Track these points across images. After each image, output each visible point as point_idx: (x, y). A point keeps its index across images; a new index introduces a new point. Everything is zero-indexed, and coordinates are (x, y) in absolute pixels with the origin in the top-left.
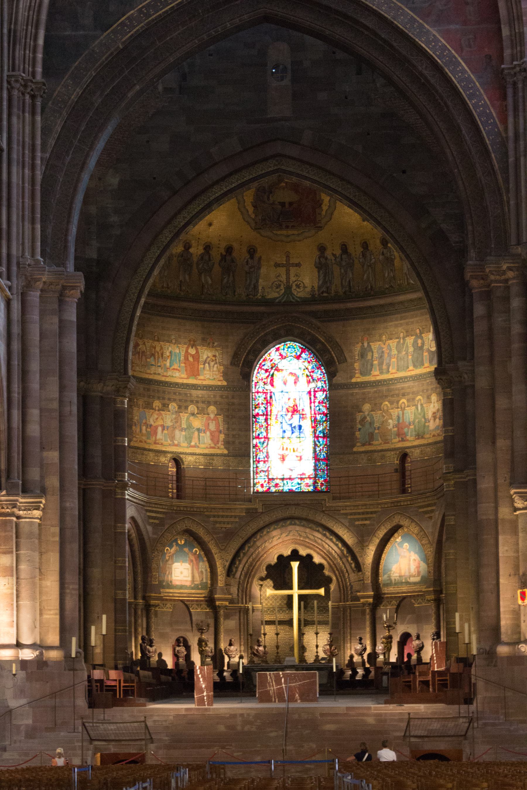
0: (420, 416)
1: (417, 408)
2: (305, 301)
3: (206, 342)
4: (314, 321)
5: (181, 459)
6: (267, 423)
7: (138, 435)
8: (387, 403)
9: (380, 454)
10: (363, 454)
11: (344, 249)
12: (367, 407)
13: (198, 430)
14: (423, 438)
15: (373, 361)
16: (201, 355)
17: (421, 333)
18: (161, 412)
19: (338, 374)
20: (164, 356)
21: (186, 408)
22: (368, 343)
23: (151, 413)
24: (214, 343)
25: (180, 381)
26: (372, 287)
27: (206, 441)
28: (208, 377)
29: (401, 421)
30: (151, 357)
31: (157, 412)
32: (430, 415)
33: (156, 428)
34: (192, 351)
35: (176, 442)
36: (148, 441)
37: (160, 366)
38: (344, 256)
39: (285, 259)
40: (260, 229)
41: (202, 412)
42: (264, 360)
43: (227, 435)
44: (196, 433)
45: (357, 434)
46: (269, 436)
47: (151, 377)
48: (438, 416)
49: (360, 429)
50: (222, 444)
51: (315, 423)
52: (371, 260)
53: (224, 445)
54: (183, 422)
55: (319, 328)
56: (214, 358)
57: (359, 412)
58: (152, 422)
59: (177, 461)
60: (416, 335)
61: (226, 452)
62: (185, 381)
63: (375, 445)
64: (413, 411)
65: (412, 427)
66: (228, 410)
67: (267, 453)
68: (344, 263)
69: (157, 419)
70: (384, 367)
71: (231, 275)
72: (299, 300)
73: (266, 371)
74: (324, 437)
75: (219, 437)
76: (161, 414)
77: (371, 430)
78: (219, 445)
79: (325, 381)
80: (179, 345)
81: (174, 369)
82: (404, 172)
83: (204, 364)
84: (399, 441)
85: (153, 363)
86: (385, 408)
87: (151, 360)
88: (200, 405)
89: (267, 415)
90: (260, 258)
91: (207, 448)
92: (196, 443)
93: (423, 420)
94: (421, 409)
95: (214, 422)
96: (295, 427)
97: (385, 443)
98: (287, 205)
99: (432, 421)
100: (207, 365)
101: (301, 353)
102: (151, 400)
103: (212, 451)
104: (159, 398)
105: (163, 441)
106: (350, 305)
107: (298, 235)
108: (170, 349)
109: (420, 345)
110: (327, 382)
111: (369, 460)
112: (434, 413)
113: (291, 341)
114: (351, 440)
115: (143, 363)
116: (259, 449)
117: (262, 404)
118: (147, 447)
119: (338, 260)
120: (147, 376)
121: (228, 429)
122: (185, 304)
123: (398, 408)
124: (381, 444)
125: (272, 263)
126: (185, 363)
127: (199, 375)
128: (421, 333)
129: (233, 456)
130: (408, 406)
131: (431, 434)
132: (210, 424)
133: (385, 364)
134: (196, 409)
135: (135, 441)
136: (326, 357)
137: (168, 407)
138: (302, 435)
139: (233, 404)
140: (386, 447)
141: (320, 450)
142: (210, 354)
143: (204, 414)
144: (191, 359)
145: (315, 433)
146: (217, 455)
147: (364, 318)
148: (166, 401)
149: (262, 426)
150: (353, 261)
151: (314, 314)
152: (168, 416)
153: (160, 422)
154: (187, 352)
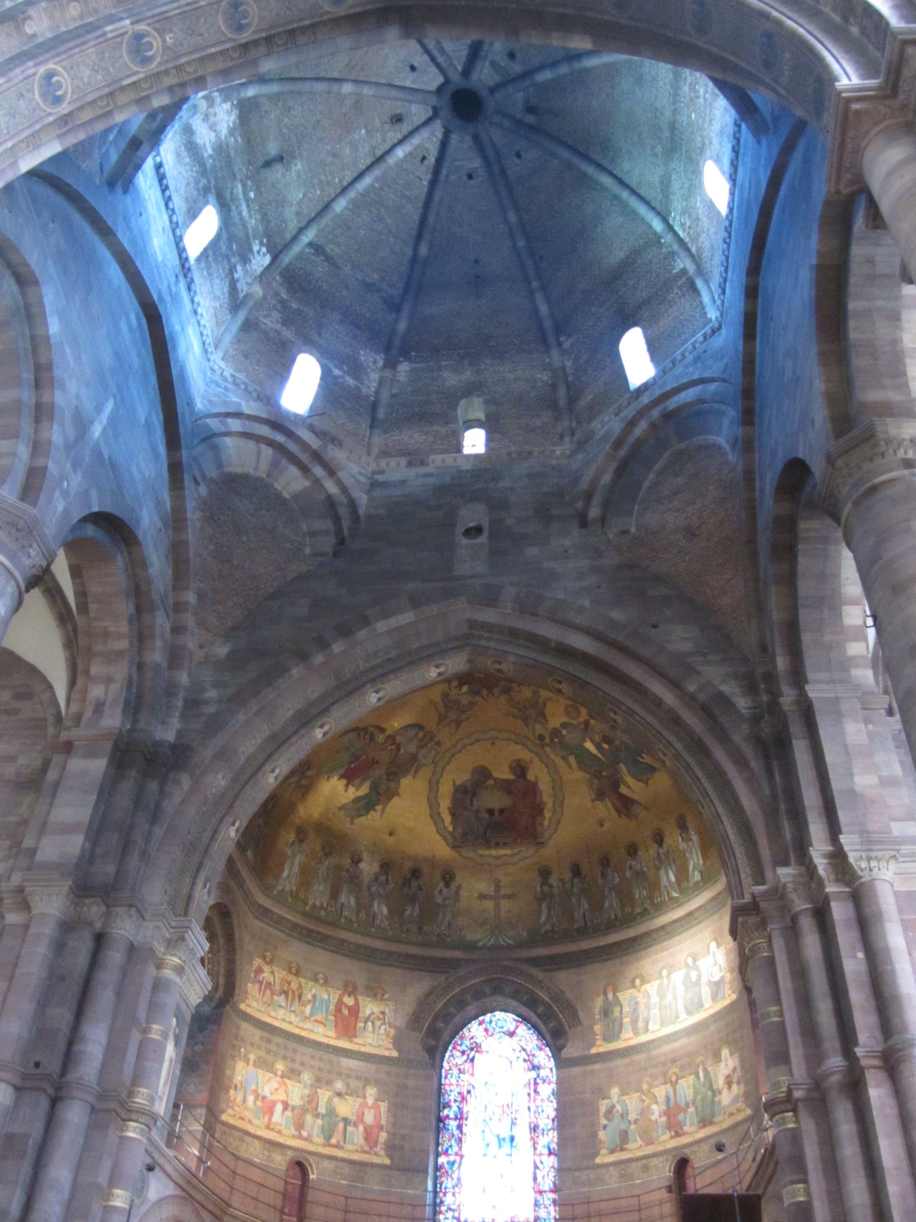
0: (703, 1089)
1: (698, 1077)
2: (521, 945)
3: (374, 992)
4: (534, 971)
5: (311, 1165)
6: (461, 1132)
7: (239, 1107)
8: (647, 1079)
9: (639, 1164)
10: (611, 1168)
11: (576, 871)
12: (615, 1091)
13: (346, 1121)
14: (711, 1123)
15: (622, 1019)
16: (361, 1008)
17: (695, 960)
18: (286, 1080)
19: (569, 1044)
20: (303, 998)
21: (329, 1083)
22: (614, 993)
23: (267, 1078)
24: (383, 995)
25: (325, 1040)
26: (616, 916)
27: (355, 1140)
28: (370, 1041)
29: (672, 1103)
30: (280, 994)
31: (278, 1079)
32: (720, 1082)
33: (273, 1104)
34: (349, 1001)
35: (304, 1134)
36: (256, 1121)
37: (294, 1012)
38: (576, 881)
39: (493, 889)
40: (460, 847)
41: (351, 1092)
42: (462, 1038)
43: (392, 1135)
44: (341, 1126)
45: (602, 1135)
46: (464, 1152)
47: (275, 1023)
48: (735, 1080)
49: (605, 1127)
50: (381, 1148)
51: (535, 1131)
52: (614, 880)
53: (384, 1150)
54: (320, 1103)
55: (540, 982)
56: (381, 1016)
57: (603, 1099)
58: (266, 1091)
59: (300, 1166)
60: (687, 965)
61: (387, 1161)
62: (332, 1042)
63: (631, 1150)
64: (691, 1082)
65: (691, 1110)
66: (397, 1095)
67: (459, 1179)
68: (576, 891)
69: (276, 1089)
70: (641, 1024)
71: (417, 906)
72: (511, 942)
73: (463, 1053)
74: (550, 1153)
75: (378, 1136)
76: (286, 1084)
77: (623, 1126)
78: (378, 1149)
79: (551, 1069)
80: (330, 989)
81: (316, 1021)
82: (655, 626)
83: (365, 1023)
84: (672, 1138)
85: (283, 1004)
86: (645, 1087)
87: (281, 999)
88: (354, 1083)
89: (461, 1118)
90: (459, 887)
91: (357, 1151)
92: (338, 1142)
93: (710, 1093)
94: (705, 1077)
95: (372, 1111)
96: (504, 1139)
97: (648, 1144)
98: (497, 813)
99: (725, 1092)
100: (370, 1024)
101: (517, 1027)
102: (270, 1058)
103: (365, 1158)
104: (285, 1058)
105: (282, 1128)
106: (586, 944)
107: (513, 855)
108: (314, 991)
109: (694, 979)
110: (554, 1070)
111: (622, 1176)
112: (728, 1077)
113: (501, 1010)
114: (592, 1145)
115: (265, 999)
116: (447, 1172)
117: (455, 1101)
118: (252, 1130)
119: (568, 886)
120: (269, 1020)
121: (394, 1125)
122: (345, 935)
123: (665, 1083)
124: (641, 1146)
125: (476, 895)
126: (335, 1016)
127: (355, 1036)
128: (695, 960)
129: (399, 1170)
130: (682, 1077)
131: (725, 1113)
132: (366, 1113)
133: (641, 1019)
134: (345, 1087)
135: (230, 1115)
136: (552, 1025)
137: (299, 1073)
138: (514, 1151)
139: (405, 1087)
140: (650, 1150)
141: (543, 1177)
142: (376, 1010)
143: (358, 1097)
144: (345, 1012)
145: (535, 1149)
146: (373, 1165)
147: (607, 960)
148: (297, 1066)
149: (453, 1135)
150: (589, 885)
151: (534, 962)
152: (296, 1089)
153: (281, 1096)
154: (340, 1000)
